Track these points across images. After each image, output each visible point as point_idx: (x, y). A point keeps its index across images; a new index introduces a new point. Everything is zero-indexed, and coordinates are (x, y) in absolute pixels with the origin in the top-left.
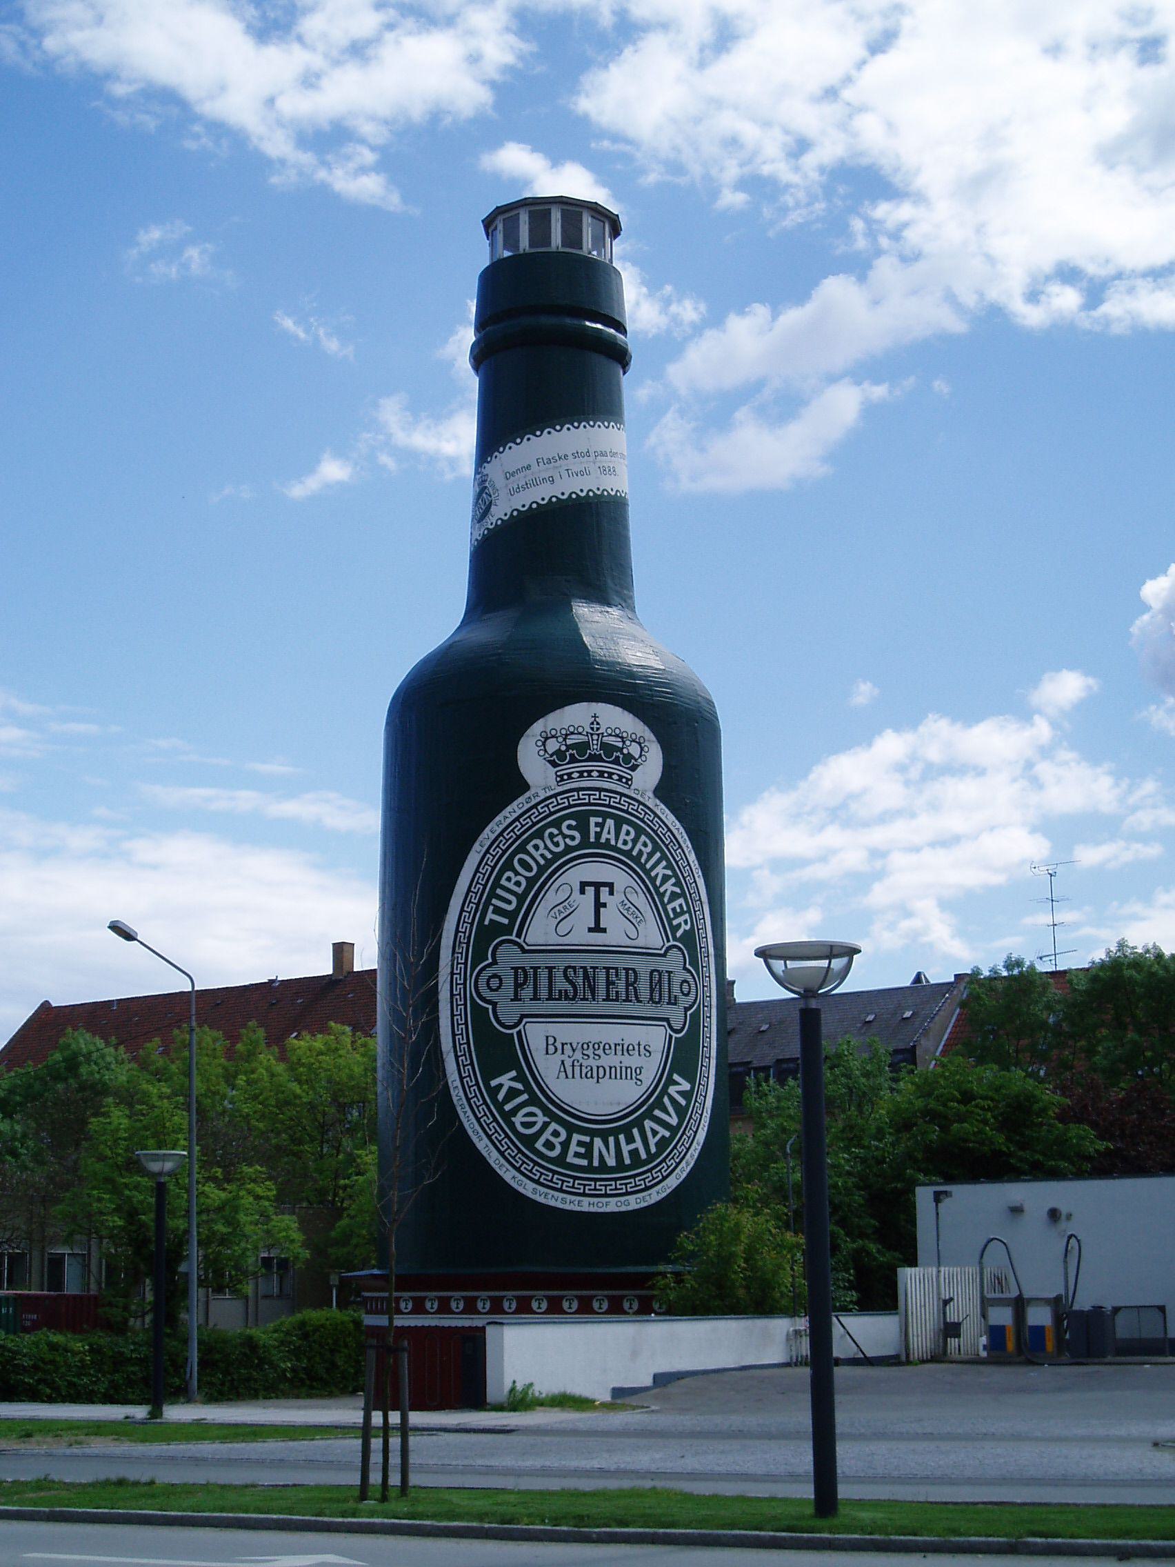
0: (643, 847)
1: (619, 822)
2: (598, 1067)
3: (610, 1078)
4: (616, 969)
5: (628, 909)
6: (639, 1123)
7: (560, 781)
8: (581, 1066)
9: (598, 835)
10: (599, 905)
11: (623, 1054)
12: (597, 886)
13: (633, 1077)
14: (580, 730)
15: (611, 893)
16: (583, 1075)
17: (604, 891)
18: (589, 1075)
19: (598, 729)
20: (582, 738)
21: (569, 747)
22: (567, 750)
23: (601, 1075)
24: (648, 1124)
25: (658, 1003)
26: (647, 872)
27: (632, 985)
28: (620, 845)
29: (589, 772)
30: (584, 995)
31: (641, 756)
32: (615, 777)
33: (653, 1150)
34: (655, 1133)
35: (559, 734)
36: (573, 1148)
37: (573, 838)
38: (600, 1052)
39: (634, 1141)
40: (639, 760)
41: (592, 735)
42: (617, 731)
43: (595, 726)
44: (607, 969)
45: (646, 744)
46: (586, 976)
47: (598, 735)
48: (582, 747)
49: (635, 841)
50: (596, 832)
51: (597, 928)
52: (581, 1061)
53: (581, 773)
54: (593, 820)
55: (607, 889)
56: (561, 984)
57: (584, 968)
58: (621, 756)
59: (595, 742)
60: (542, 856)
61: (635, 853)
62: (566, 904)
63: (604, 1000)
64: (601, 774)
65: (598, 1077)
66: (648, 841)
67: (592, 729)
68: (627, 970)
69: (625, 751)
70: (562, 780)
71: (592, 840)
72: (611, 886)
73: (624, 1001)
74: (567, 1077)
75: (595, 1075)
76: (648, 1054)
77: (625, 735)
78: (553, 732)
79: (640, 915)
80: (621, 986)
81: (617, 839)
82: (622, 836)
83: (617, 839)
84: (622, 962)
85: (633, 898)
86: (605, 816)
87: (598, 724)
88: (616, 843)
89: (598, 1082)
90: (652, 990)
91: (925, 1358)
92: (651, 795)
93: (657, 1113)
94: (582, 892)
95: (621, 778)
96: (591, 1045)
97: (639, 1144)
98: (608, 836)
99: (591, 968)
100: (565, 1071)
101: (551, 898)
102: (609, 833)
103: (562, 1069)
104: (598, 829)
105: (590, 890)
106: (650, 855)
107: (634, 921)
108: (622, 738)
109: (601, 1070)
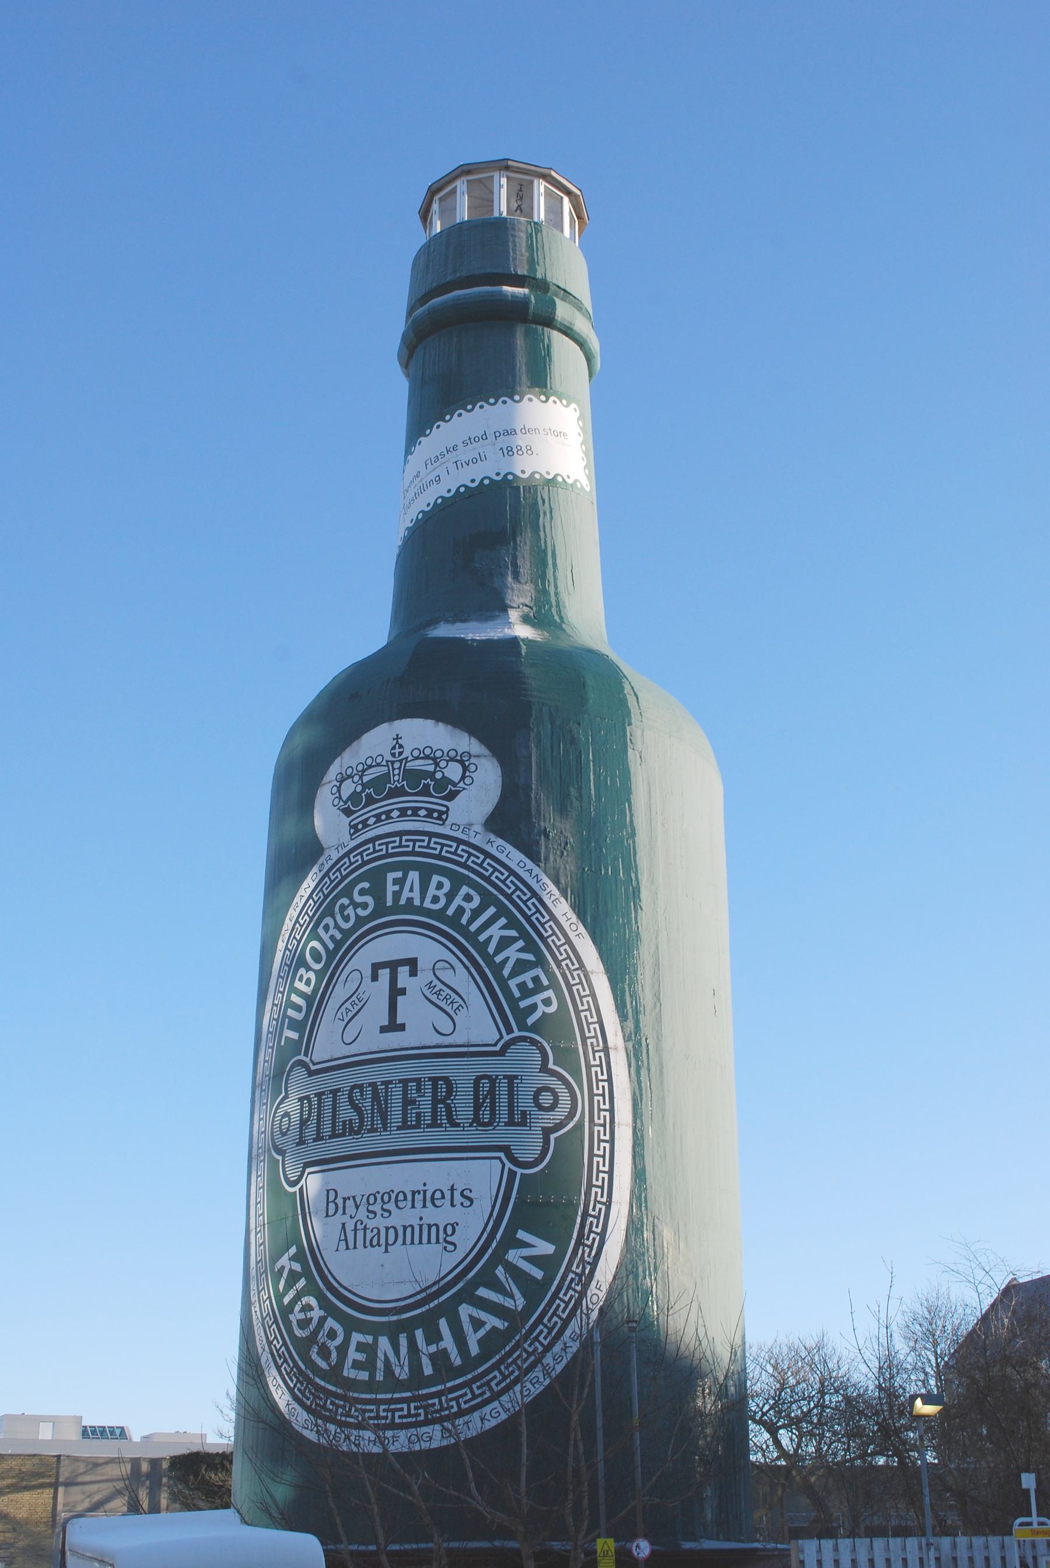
2: (387, 1229)
3: (404, 1243)
4: (418, 1081)
5: (438, 993)
6: (450, 1312)
7: (354, 833)
8: (365, 1229)
9: (397, 895)
10: (396, 992)
11: (424, 1206)
13: (441, 1240)
14: (379, 760)
15: (413, 973)
16: (368, 1244)
17: (403, 971)
18: (375, 1242)
19: (400, 754)
20: (383, 770)
21: (365, 786)
22: (363, 791)
23: (391, 1240)
24: (465, 1311)
28: (427, 904)
30: (372, 1125)
33: (474, 1350)
34: (477, 1324)
35: (355, 772)
36: (353, 1355)
37: (365, 906)
38: (391, 1206)
39: (440, 1338)
41: (393, 763)
42: (428, 751)
43: (397, 751)
47: (401, 761)
49: (450, 896)
50: (393, 892)
51: (394, 1026)
52: (366, 1221)
54: (391, 876)
55: (407, 968)
56: (346, 1113)
57: (373, 1085)
59: (396, 772)
60: (332, 938)
61: (450, 912)
62: (354, 998)
63: (399, 1128)
65: (387, 1244)
67: (393, 755)
69: (439, 776)
70: (357, 830)
71: (389, 903)
72: (412, 964)
73: (429, 1126)
74: (348, 1248)
75: (383, 1241)
76: (467, 1203)
77: (439, 754)
81: (423, 898)
82: (432, 891)
83: (423, 898)
85: (446, 976)
87: (401, 746)
88: (422, 902)
89: (386, 1251)
90: (477, 1107)
93: (483, 1292)
94: (375, 978)
96: (379, 1197)
97: (448, 1342)
98: (411, 895)
99: (383, 1083)
100: (346, 1240)
102: (411, 890)
103: (343, 1237)
105: (384, 974)
108: (434, 759)
109: (392, 1232)
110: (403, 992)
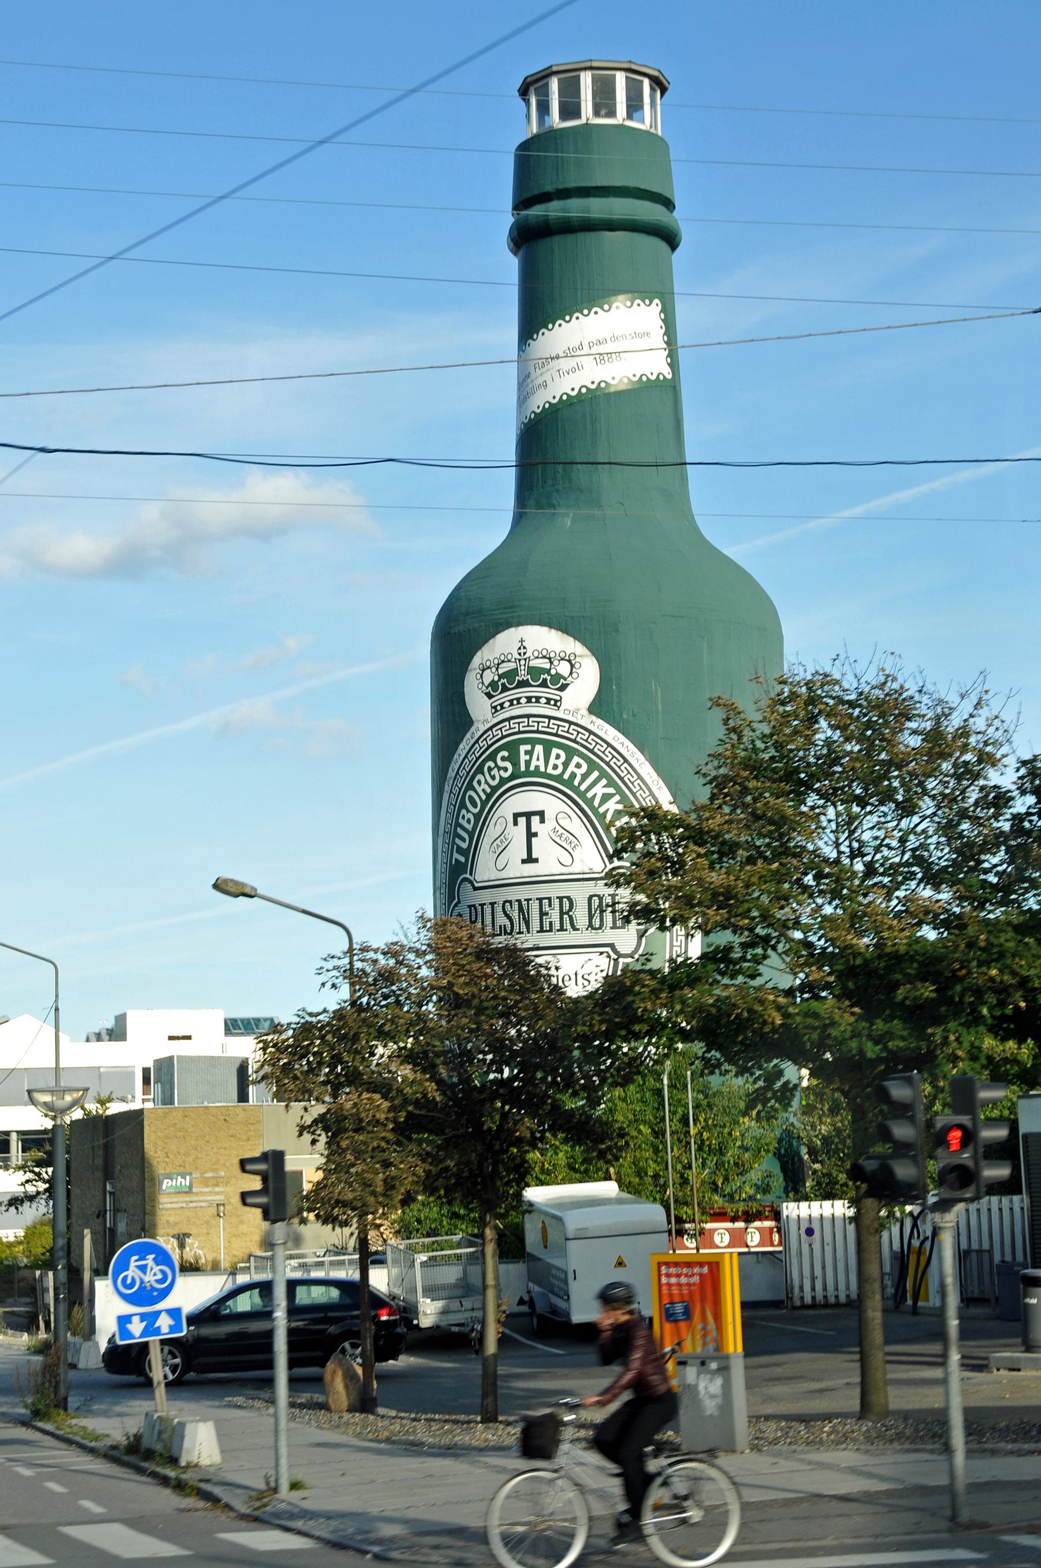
0: (577, 768)
1: (548, 746)
4: (549, 899)
5: (561, 836)
9: (528, 763)
10: (531, 835)
12: (528, 815)
14: (509, 657)
15: (542, 821)
19: (525, 653)
20: (512, 666)
21: (500, 677)
22: (499, 680)
25: (600, 928)
26: (582, 795)
27: (567, 913)
28: (550, 771)
29: (518, 700)
31: (571, 673)
32: (543, 700)
37: (506, 769)
40: (570, 679)
42: (544, 653)
43: (522, 651)
44: (540, 900)
45: (578, 659)
46: (521, 909)
48: (511, 674)
49: (566, 765)
50: (526, 761)
51: (530, 859)
53: (511, 701)
54: (523, 748)
57: (519, 901)
58: (549, 678)
60: (484, 790)
61: (566, 776)
64: (529, 699)
66: (581, 761)
67: (520, 654)
68: (561, 899)
69: (553, 672)
70: (496, 711)
71: (523, 768)
72: (541, 814)
77: (552, 655)
78: (488, 664)
79: (574, 840)
80: (555, 916)
82: (552, 761)
84: (554, 891)
86: (533, 742)
91: (808, 1300)
92: (585, 712)
94: (516, 823)
95: (548, 700)
98: (537, 763)
101: (492, 832)
102: (538, 759)
104: (527, 757)
105: (522, 821)
106: (585, 777)
107: (568, 847)
108: (550, 658)
110: (536, 835)
